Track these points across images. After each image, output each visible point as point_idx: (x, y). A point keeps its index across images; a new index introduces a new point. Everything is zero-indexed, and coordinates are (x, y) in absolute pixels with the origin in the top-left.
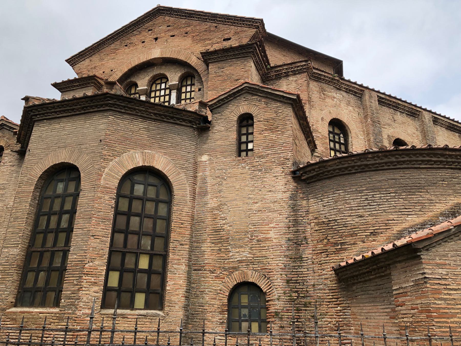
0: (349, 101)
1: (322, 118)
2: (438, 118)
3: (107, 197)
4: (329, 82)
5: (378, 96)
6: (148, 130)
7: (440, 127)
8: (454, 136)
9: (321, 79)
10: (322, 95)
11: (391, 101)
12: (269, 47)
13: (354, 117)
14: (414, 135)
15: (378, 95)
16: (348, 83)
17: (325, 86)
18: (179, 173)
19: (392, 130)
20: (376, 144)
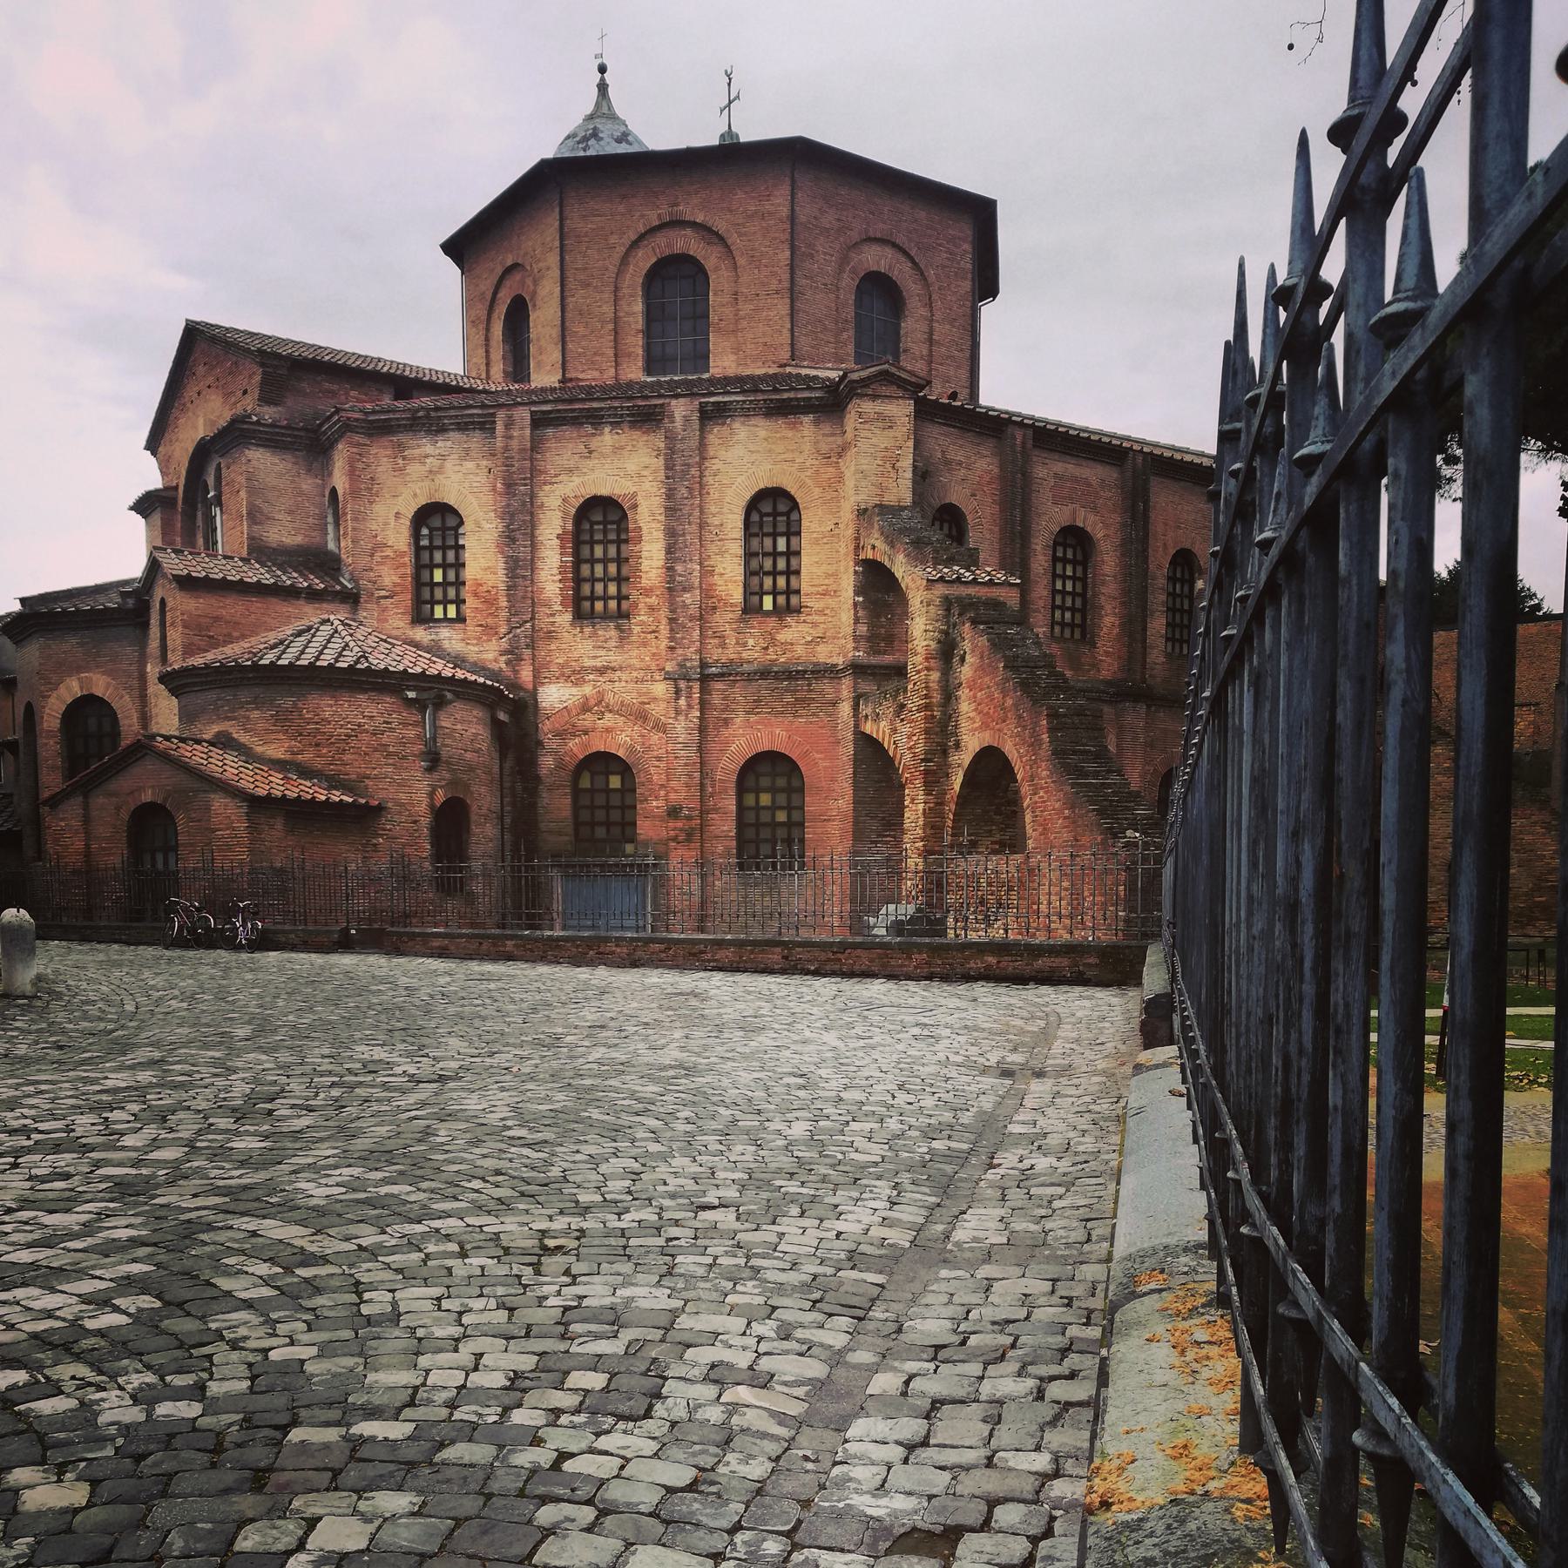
0: (467, 451)
3: (52, 742)
4: (412, 425)
5: (532, 412)
6: (82, 644)
8: (793, 427)
10: (400, 461)
11: (573, 410)
14: (644, 473)
15: (533, 409)
16: (453, 413)
17: (402, 438)
18: (122, 697)
20: (508, 537)
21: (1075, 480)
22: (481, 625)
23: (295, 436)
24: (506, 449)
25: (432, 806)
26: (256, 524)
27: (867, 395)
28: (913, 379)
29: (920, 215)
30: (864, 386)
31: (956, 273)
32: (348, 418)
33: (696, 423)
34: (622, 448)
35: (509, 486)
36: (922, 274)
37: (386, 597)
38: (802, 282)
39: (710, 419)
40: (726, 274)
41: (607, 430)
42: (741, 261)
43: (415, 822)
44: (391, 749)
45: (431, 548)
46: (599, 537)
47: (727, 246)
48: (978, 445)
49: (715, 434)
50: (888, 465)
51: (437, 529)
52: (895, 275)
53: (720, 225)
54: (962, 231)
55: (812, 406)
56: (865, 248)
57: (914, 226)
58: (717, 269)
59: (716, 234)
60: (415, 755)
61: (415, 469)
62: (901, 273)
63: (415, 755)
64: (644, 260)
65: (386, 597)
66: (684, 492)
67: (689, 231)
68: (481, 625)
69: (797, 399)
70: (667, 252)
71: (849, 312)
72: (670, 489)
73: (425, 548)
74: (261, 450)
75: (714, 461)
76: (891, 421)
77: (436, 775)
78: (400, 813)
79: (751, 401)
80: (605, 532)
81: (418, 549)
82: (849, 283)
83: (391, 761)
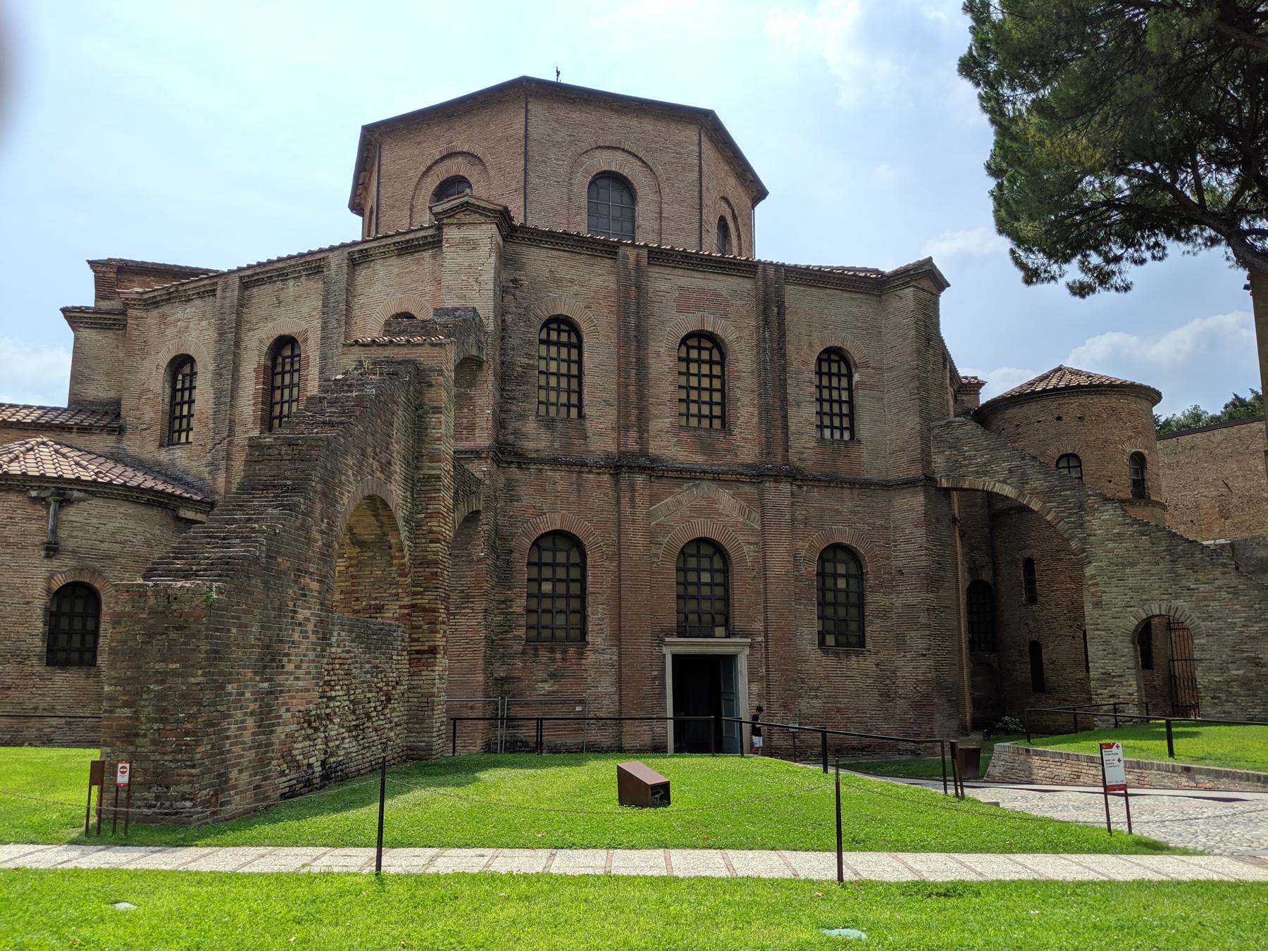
1: (158, 365)
2: (366, 250)
4: (169, 299)
5: (241, 277)
7: (381, 261)
8: (418, 261)
9: (158, 302)
11: (267, 272)
12: (389, 141)
13: (206, 337)
14: (314, 313)
17: (166, 309)
19: (270, 325)
20: (217, 374)
21: (702, 291)
22: (201, 445)
23: (114, 320)
24: (222, 307)
25: (48, 590)
26: (78, 383)
27: (452, 224)
28: (490, 207)
29: (648, 126)
30: (449, 217)
31: (683, 168)
32: (127, 299)
33: (345, 270)
34: (300, 296)
35: (221, 334)
36: (651, 170)
37: (146, 429)
38: (534, 180)
39: (359, 264)
40: (483, 183)
41: (291, 283)
42: (492, 173)
43: (28, 603)
44: (12, 540)
45: (183, 390)
46: (288, 368)
47: (484, 165)
48: (592, 265)
49: (363, 274)
50: (471, 280)
51: (187, 375)
52: (625, 172)
53: (479, 151)
54: (689, 135)
55: (430, 243)
56: (597, 153)
57: (642, 135)
58: (478, 181)
59: (476, 157)
60: (36, 545)
61: (170, 331)
62: (630, 169)
63: (36, 545)
64: (432, 183)
65: (146, 429)
66: (334, 322)
67: (460, 159)
68: (201, 445)
69: (417, 239)
70: (446, 176)
71: (584, 200)
72: (325, 323)
73: (179, 390)
74: (88, 330)
75: (361, 297)
76: (474, 244)
77: (56, 563)
78: (12, 596)
79: (384, 246)
80: (292, 364)
81: (174, 390)
82: (581, 181)
83: (8, 551)
